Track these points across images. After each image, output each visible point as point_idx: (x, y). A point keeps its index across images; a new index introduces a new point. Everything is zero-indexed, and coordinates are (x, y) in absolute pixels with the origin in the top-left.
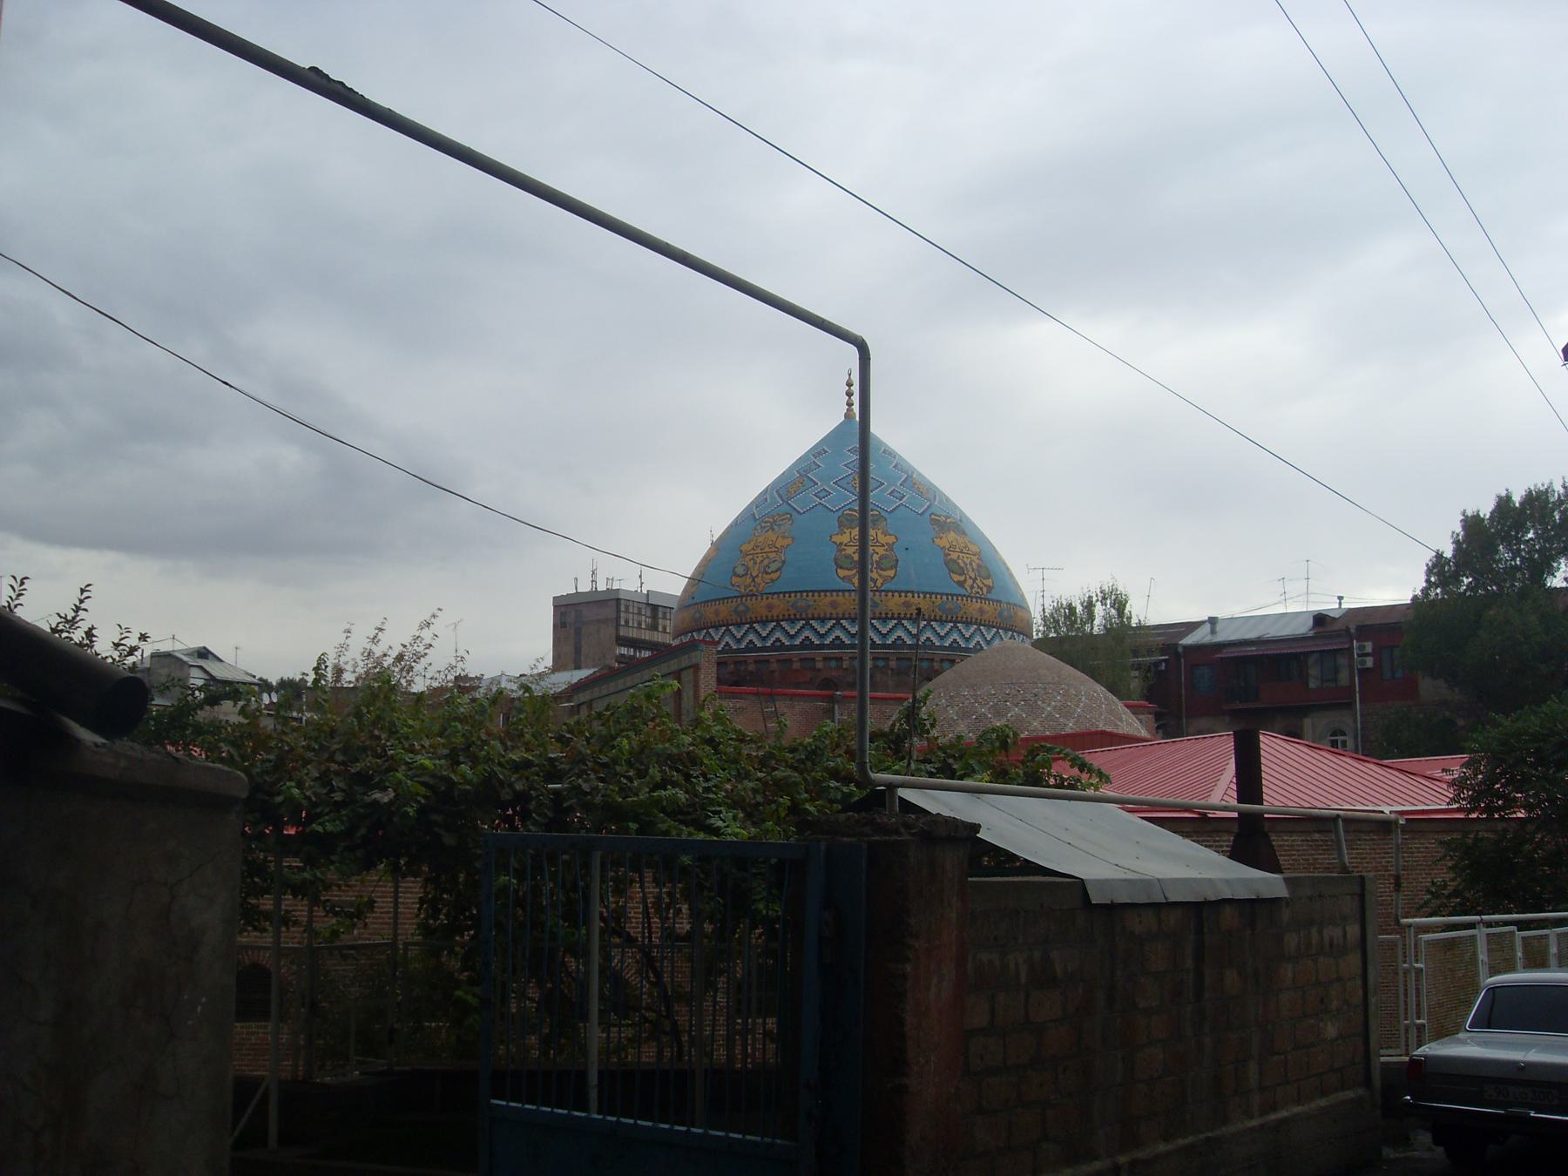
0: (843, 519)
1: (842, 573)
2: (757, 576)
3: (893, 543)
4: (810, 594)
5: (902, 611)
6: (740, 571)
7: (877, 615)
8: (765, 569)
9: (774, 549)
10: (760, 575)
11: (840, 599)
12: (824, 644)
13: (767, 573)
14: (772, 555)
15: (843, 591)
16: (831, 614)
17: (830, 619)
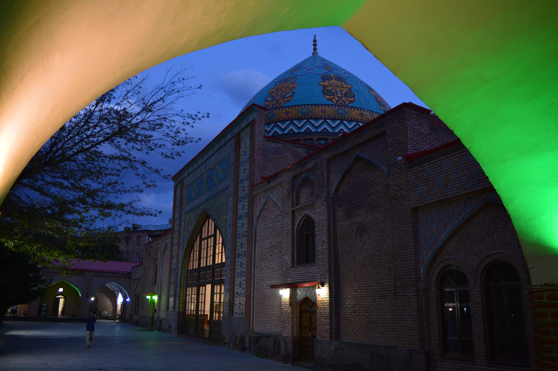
0: (323, 77)
1: (327, 97)
2: (279, 100)
3: (351, 88)
4: (310, 106)
5: (359, 117)
6: (269, 99)
7: (346, 118)
8: (283, 96)
9: (288, 88)
10: (281, 99)
11: (327, 109)
12: (318, 132)
13: (285, 98)
14: (287, 91)
15: (328, 105)
16: (322, 116)
17: (321, 119)
